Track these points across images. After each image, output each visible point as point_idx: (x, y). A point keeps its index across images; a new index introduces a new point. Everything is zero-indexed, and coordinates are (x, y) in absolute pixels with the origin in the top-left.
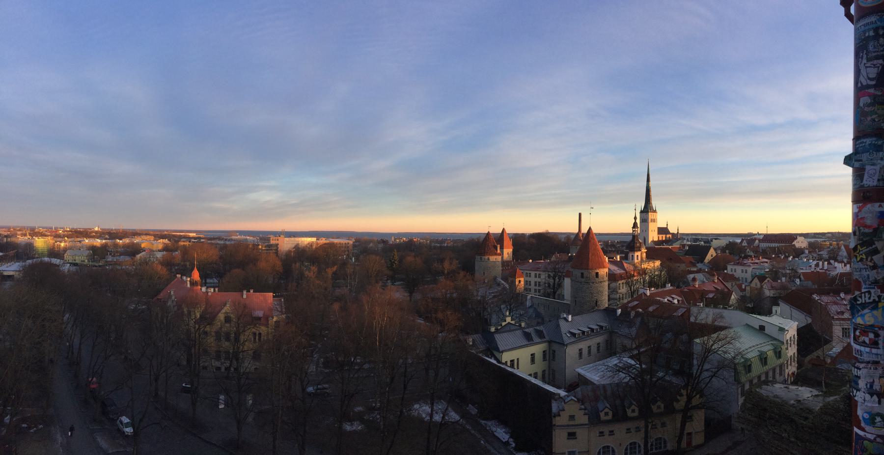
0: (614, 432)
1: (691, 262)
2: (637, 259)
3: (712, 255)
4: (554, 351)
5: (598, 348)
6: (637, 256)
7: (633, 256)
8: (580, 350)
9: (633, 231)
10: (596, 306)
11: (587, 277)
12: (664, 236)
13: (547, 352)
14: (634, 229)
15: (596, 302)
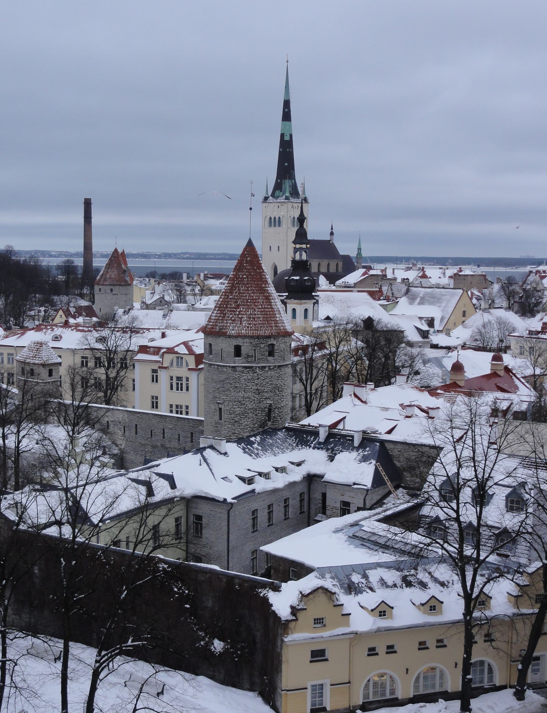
0: (395, 647)
1: (418, 329)
2: (306, 317)
3: (464, 312)
4: (199, 518)
5: (286, 507)
6: (306, 310)
7: (294, 310)
8: (254, 512)
9: (296, 250)
10: (269, 420)
11: (248, 356)
12: (324, 263)
13: (183, 521)
14: (298, 246)
15: (270, 410)
